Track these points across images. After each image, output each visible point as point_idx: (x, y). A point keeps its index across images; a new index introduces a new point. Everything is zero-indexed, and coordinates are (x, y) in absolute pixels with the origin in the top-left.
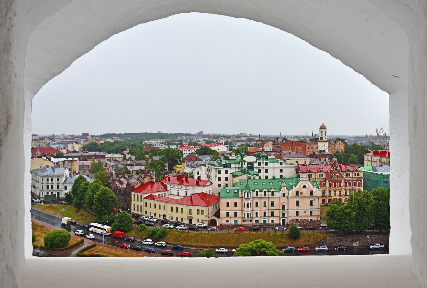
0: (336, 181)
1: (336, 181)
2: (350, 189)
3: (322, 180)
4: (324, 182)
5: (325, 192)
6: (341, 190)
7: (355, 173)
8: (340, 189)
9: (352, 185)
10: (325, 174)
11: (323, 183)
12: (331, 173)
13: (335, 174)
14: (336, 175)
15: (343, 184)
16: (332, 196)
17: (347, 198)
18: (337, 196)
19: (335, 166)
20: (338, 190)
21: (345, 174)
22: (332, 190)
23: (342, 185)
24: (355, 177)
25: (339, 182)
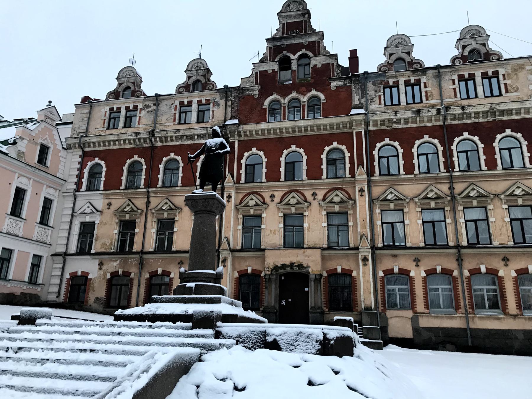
0: (299, 141)
1: (299, 141)
3: (196, 142)
6: (342, 201)
7: (461, 78)
8: (337, 199)
9: (449, 166)
10: (222, 102)
12: (265, 92)
13: (294, 94)
14: (304, 99)
16: (263, 250)
17: (404, 272)
18: (309, 251)
19: (294, 49)
20: (315, 204)
24: (465, 103)
25: (327, 149)
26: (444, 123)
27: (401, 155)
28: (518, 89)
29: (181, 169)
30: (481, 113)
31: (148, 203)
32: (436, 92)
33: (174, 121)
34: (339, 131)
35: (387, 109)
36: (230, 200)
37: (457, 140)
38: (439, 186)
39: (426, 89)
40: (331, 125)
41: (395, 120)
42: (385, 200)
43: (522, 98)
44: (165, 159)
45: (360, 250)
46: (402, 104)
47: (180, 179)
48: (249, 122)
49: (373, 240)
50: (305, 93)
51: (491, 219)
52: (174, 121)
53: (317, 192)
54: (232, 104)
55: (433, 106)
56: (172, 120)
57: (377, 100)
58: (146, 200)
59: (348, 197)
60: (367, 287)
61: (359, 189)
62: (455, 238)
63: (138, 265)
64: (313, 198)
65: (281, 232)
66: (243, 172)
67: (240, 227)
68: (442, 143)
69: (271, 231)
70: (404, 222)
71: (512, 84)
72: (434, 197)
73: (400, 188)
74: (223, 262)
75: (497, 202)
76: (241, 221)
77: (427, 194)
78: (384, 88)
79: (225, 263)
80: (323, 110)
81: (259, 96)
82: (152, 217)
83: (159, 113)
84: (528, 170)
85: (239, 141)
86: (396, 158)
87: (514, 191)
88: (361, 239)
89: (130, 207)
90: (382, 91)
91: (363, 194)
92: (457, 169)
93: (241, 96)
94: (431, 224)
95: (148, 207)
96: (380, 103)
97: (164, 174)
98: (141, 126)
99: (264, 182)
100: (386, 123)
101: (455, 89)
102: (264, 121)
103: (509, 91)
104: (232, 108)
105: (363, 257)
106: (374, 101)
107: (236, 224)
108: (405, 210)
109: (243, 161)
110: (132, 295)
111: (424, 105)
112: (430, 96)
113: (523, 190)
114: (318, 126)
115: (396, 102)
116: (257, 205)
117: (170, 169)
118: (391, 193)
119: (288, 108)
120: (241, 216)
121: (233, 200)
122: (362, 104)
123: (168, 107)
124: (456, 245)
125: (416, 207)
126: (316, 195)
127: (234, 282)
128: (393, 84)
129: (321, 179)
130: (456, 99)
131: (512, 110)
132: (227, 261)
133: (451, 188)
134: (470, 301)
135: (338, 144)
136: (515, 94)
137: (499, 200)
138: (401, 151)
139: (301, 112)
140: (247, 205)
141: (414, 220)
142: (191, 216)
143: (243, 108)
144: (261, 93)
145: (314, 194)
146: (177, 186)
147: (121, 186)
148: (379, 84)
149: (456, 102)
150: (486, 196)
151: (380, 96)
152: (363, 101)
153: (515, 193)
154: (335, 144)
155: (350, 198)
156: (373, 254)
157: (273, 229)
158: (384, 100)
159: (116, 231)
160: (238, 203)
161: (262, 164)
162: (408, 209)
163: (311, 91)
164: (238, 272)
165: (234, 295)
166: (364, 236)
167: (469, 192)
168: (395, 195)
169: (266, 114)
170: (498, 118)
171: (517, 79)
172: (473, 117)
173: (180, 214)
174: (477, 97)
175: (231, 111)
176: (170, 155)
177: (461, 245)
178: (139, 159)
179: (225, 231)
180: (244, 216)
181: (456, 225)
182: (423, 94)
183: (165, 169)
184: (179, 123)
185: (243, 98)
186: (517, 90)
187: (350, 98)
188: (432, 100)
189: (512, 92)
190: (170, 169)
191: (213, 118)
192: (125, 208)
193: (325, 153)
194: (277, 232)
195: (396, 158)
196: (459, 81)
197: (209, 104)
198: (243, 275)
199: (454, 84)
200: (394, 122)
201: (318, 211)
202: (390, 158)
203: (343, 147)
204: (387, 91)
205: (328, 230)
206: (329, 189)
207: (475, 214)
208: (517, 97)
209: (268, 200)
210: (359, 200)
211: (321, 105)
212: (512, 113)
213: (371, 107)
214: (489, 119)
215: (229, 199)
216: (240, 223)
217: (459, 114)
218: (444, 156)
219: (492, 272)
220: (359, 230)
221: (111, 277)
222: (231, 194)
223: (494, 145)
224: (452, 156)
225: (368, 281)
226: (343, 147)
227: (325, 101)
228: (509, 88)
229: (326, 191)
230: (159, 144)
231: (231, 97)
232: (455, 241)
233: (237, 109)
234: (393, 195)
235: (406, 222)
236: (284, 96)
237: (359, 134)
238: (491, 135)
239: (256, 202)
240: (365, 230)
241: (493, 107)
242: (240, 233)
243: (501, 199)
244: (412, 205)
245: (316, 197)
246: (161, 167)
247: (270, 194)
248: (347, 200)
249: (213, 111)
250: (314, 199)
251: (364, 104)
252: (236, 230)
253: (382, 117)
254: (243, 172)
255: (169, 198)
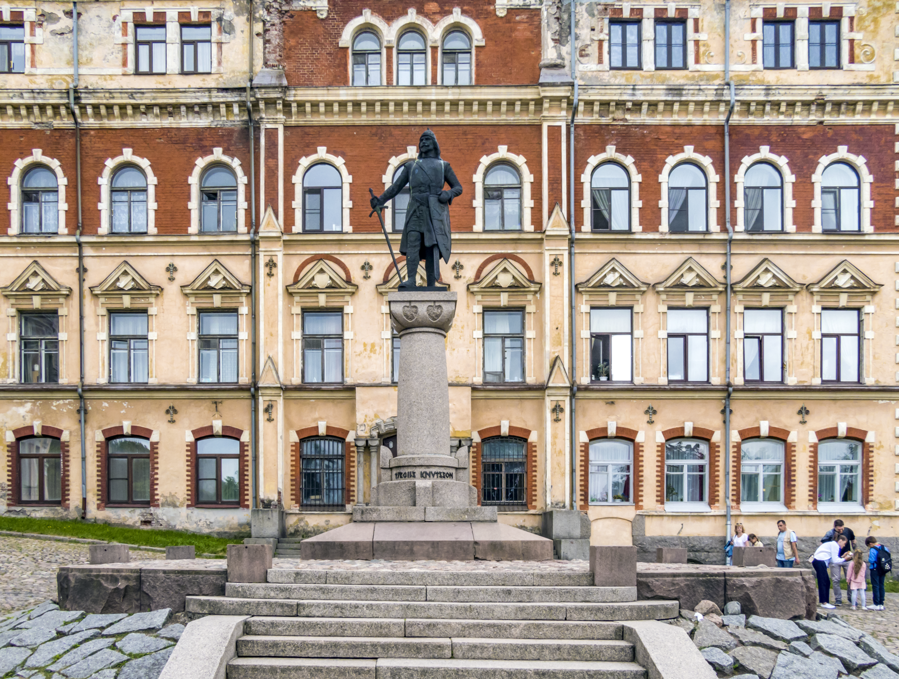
2: (689, 279)
4: (218, 154)
5: (244, 310)
6: (516, 288)
8: (505, 280)
10: (240, 22)
11: (201, 163)
13: (412, 16)
14: (435, 33)
15: (555, 183)
16: (351, 389)
21: (584, 33)
22: (367, 289)
23: (537, 211)
24: (772, 77)
25: (486, 160)
26: (728, 120)
27: (635, 188)
28: (873, 54)
29: (151, 190)
30: (799, 104)
31: (82, 270)
32: (715, 46)
33: (125, 64)
34: (511, 119)
35: (615, 77)
36: (274, 271)
37: (747, 160)
38: (704, 261)
39: (697, 36)
40: (497, 103)
41: (629, 105)
42: (602, 287)
43: (878, 77)
44: (110, 163)
45: (547, 392)
46: (645, 67)
47: (152, 215)
48: (309, 85)
49: (572, 368)
50: (437, 17)
51: (790, 333)
52: (125, 64)
53: (463, 261)
54: (266, 31)
55: (710, 78)
56: (120, 62)
57: (593, 50)
58: (75, 263)
59: (526, 275)
60: (559, 464)
61: (553, 258)
62: (723, 369)
63: (77, 415)
64: (454, 274)
65: (388, 348)
66: (297, 204)
67: (297, 334)
68: (720, 170)
69: (365, 345)
70: (631, 333)
71: (863, 43)
72: (694, 283)
73: (629, 261)
74: (267, 410)
75: (804, 297)
76: (297, 321)
77: (682, 276)
78: (613, 22)
79: (270, 414)
80: (477, 65)
81: (329, 14)
82: (96, 305)
83: (83, 40)
84: (867, 238)
85: (286, 128)
86: (627, 192)
87: (836, 278)
88: (552, 367)
89: (39, 279)
90: (606, 31)
91: (560, 269)
92: (740, 226)
93: (286, 12)
94: (682, 339)
95: (81, 281)
96: (600, 61)
97: (112, 202)
98: (38, 71)
99: (347, 233)
100: (612, 109)
101: (754, 42)
102: (341, 79)
103: (856, 60)
104: (267, 42)
105: (554, 404)
106: (587, 55)
107: (289, 328)
108: (636, 309)
109: (297, 179)
110: (70, 478)
111: (691, 75)
112: (704, 54)
113: (852, 277)
114: (469, 103)
115: (632, 61)
116: (333, 286)
117: (124, 190)
118: (614, 270)
119: (398, 53)
120: (297, 310)
121: (279, 271)
122: (563, 59)
123: (104, 23)
124: (724, 383)
125: (658, 302)
126: (462, 267)
127: (289, 453)
128: (631, 15)
129: (472, 232)
130: (754, 67)
131: (854, 103)
132: (274, 409)
133: (724, 267)
134: (735, 488)
135: (509, 150)
136: (867, 67)
137: (808, 295)
138: (637, 178)
139: (426, 64)
140: (311, 287)
141: (651, 331)
142: (184, 305)
143: (292, 42)
144: (334, 5)
145: (457, 267)
146: (145, 234)
147: (9, 226)
148: (600, 13)
149: (754, 75)
150: (788, 287)
151: (601, 42)
152: (565, 50)
153: (836, 282)
154: (503, 152)
155: (531, 280)
156: (573, 396)
157: (369, 341)
158: (609, 53)
159: (14, 336)
160: (291, 281)
161: (341, 188)
162: (642, 306)
163: (451, 13)
164: (298, 432)
165: (292, 480)
166: (558, 362)
167: (758, 277)
168: (621, 276)
169: (346, 65)
170: (828, 119)
171: (875, 32)
172: (782, 113)
173: (160, 299)
174: (793, 66)
175: (265, 48)
176: (122, 154)
177: (732, 382)
178: (46, 160)
179: (266, 343)
180: (305, 311)
181: (728, 343)
182: (691, 46)
183: (113, 191)
184: (137, 73)
185: (292, 16)
186: (870, 57)
187: (536, 42)
188: (707, 63)
189: (862, 62)
190: (124, 190)
191: (220, 63)
192: (27, 280)
193: (481, 169)
194: (377, 348)
195: (627, 192)
196: (766, 22)
197: (208, 25)
198: (308, 437)
199: (754, 30)
200: (628, 109)
201: (465, 304)
202: (613, 192)
203: (520, 160)
204: (617, 29)
205: (483, 345)
206: (488, 256)
207: (765, 322)
208: (870, 73)
209: (357, 275)
210: (551, 285)
211: (474, 51)
212: (854, 110)
213: (581, 67)
214: (814, 118)
215: (271, 269)
216: (297, 326)
217: (759, 103)
218: (721, 195)
219: (778, 436)
220: (548, 348)
221: (18, 440)
222: (274, 258)
223: (814, 178)
224: (733, 197)
225: (560, 452)
226: (520, 160)
227: (483, 44)
228: (857, 51)
229: (483, 259)
230: (91, 122)
231: (261, 12)
232: (723, 375)
233: (279, 45)
234: (617, 275)
235: (637, 333)
236: (389, 19)
237: (554, 132)
238: (811, 156)
239: (330, 278)
240: (559, 348)
241: (824, 92)
242: (298, 347)
243: (812, 293)
244: (651, 298)
245: (461, 273)
246: (104, 181)
247: (362, 260)
248: (525, 283)
249: (220, 44)
250: (458, 277)
251: (567, 57)
252: (288, 341)
253: (605, 94)
254: (297, 204)
255: (130, 260)
